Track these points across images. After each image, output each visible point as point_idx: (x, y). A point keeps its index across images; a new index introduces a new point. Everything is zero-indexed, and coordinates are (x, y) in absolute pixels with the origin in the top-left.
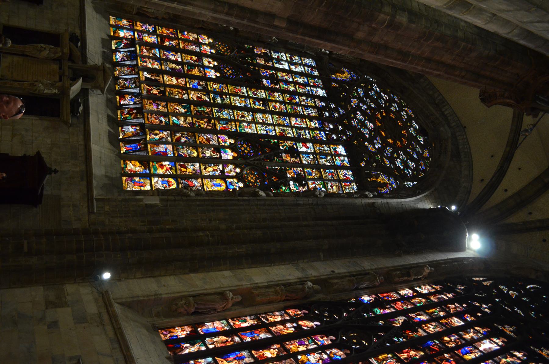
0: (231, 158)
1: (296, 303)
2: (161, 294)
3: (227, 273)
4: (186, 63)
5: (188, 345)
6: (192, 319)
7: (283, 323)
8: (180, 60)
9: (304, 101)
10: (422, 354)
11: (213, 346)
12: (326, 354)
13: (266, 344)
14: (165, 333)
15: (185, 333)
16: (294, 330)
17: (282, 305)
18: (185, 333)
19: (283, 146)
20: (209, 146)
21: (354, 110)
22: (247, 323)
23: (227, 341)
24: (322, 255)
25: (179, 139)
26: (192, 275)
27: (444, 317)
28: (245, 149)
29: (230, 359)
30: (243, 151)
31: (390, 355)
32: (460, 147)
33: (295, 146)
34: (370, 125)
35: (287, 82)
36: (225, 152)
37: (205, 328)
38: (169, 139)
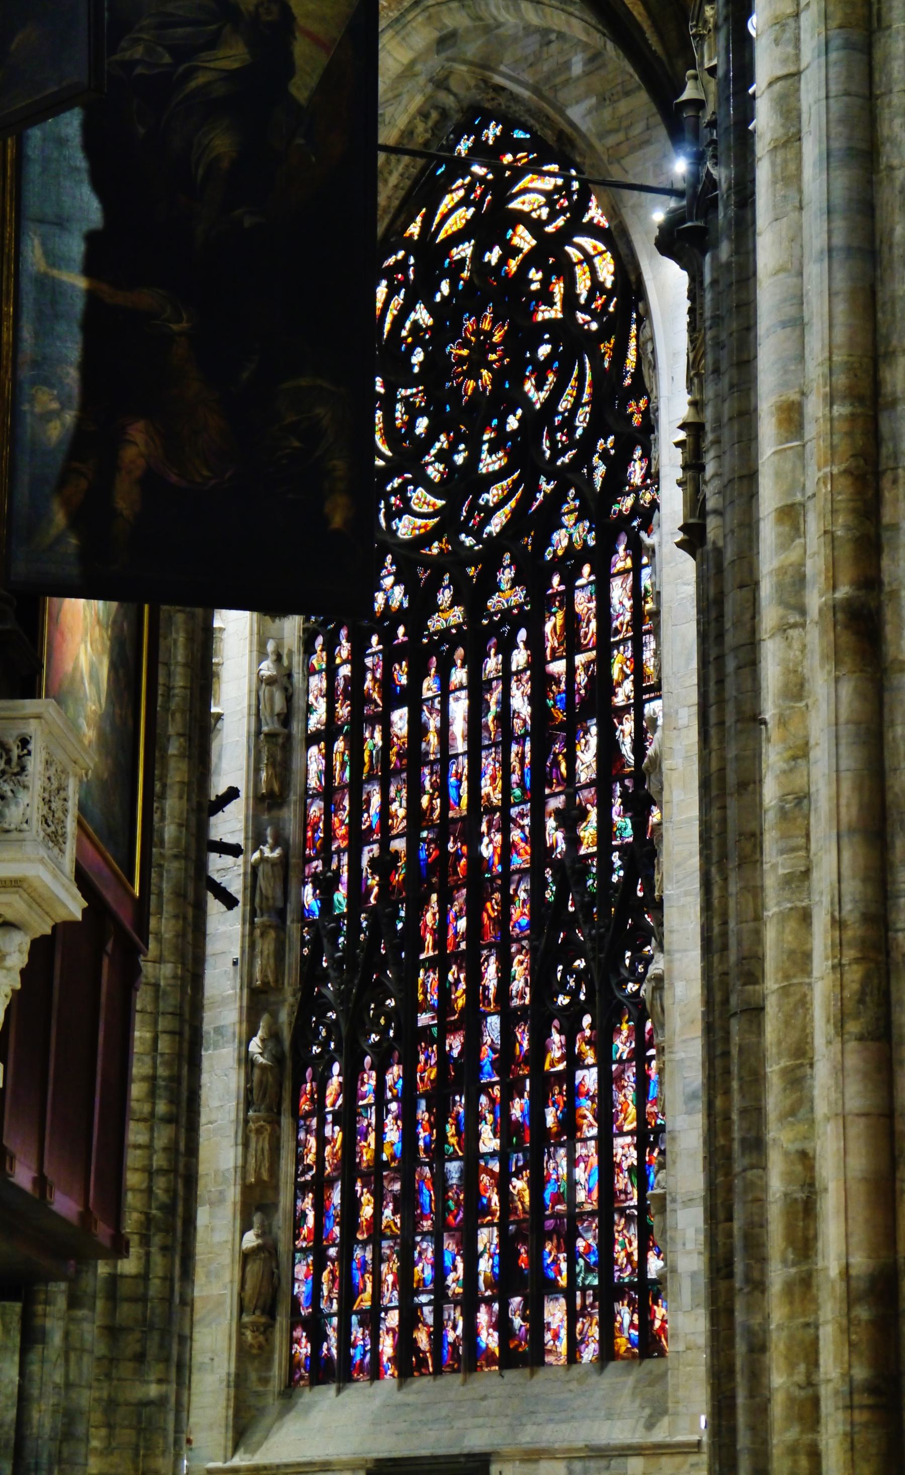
1: (288, 1085)
2: (229, 1374)
5: (325, 1345)
6: (282, 1320)
7: (323, 1141)
10: (434, 897)
11: (335, 1301)
12: (391, 1101)
13: (351, 1204)
14: (297, 1376)
15: (304, 1340)
16: (337, 1128)
17: (286, 1121)
18: (304, 1340)
22: (307, 1212)
23: (332, 1272)
27: (387, 736)
29: (361, 1286)
31: (422, 972)
37: (302, 1299)
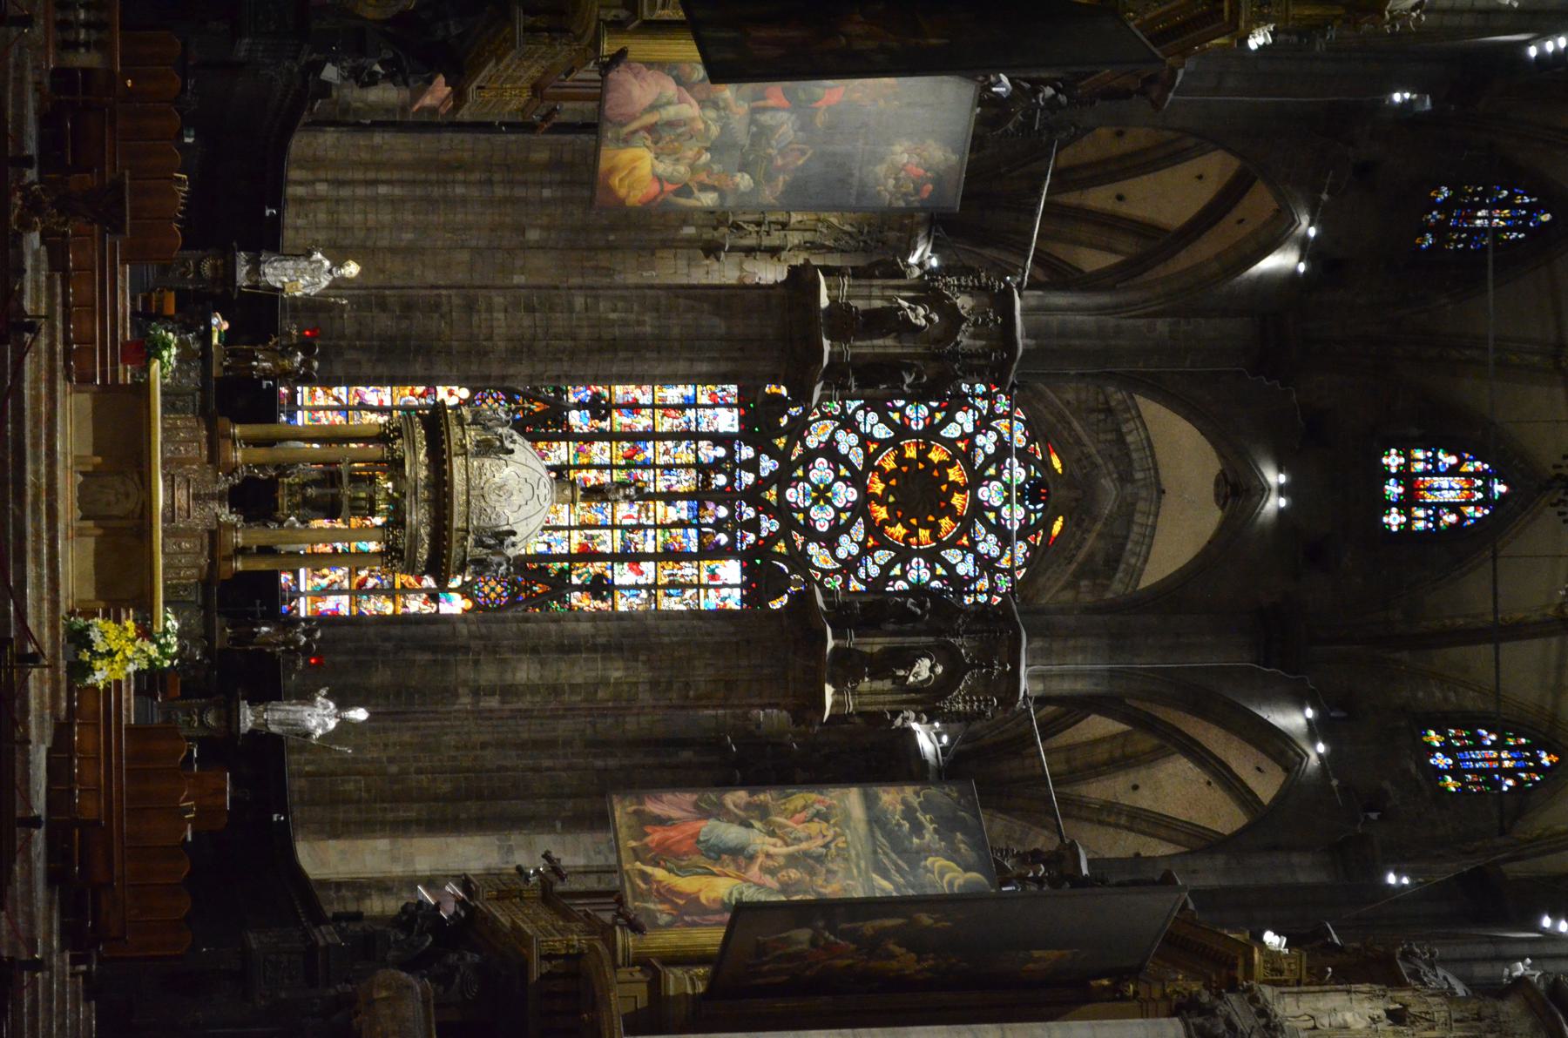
0: (459, 612)
3: (383, 844)
4: (398, 408)
8: (387, 403)
9: (667, 452)
19: (579, 576)
20: (418, 592)
21: (809, 457)
24: (559, 825)
25: (365, 581)
26: (332, 843)
28: (493, 590)
30: (487, 596)
32: (1129, 546)
33: (609, 573)
34: (845, 494)
35: (634, 407)
36: (448, 601)
38: (346, 584)
